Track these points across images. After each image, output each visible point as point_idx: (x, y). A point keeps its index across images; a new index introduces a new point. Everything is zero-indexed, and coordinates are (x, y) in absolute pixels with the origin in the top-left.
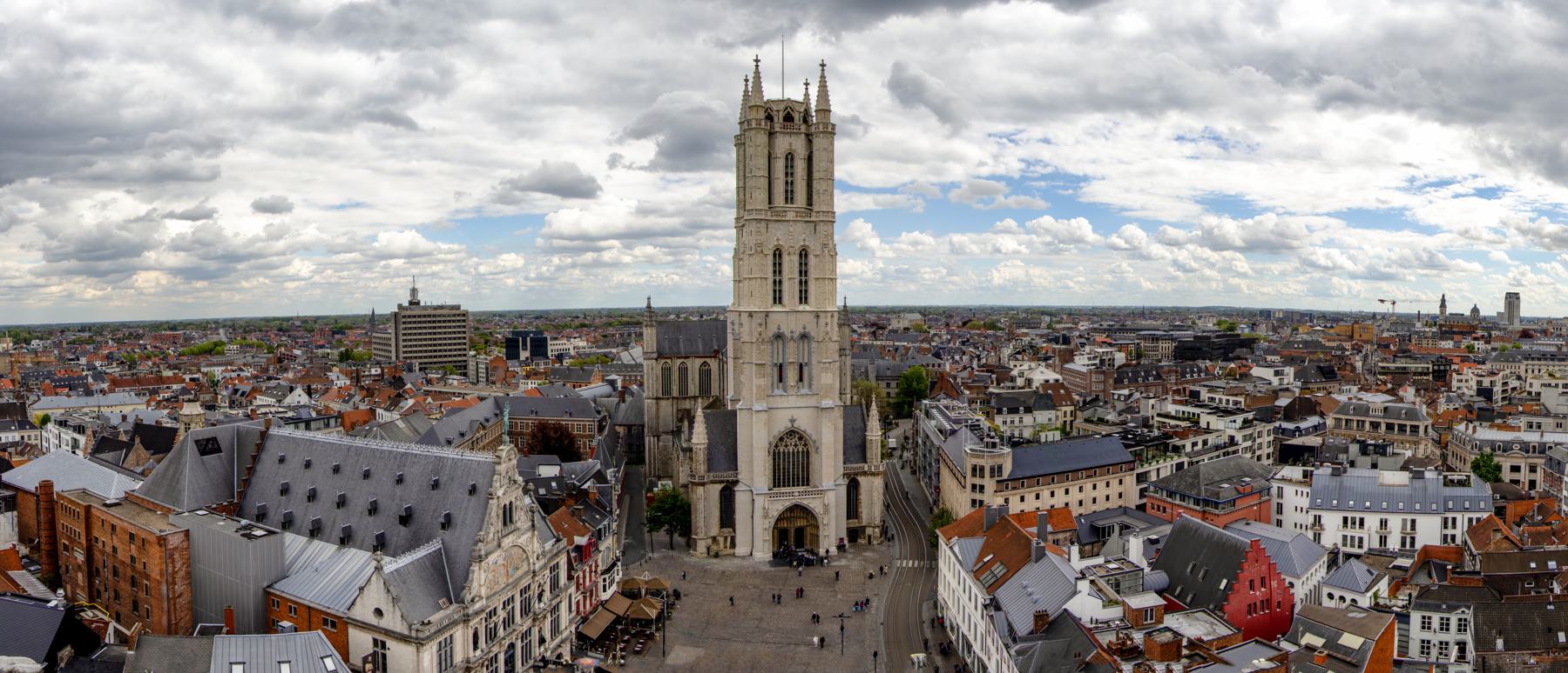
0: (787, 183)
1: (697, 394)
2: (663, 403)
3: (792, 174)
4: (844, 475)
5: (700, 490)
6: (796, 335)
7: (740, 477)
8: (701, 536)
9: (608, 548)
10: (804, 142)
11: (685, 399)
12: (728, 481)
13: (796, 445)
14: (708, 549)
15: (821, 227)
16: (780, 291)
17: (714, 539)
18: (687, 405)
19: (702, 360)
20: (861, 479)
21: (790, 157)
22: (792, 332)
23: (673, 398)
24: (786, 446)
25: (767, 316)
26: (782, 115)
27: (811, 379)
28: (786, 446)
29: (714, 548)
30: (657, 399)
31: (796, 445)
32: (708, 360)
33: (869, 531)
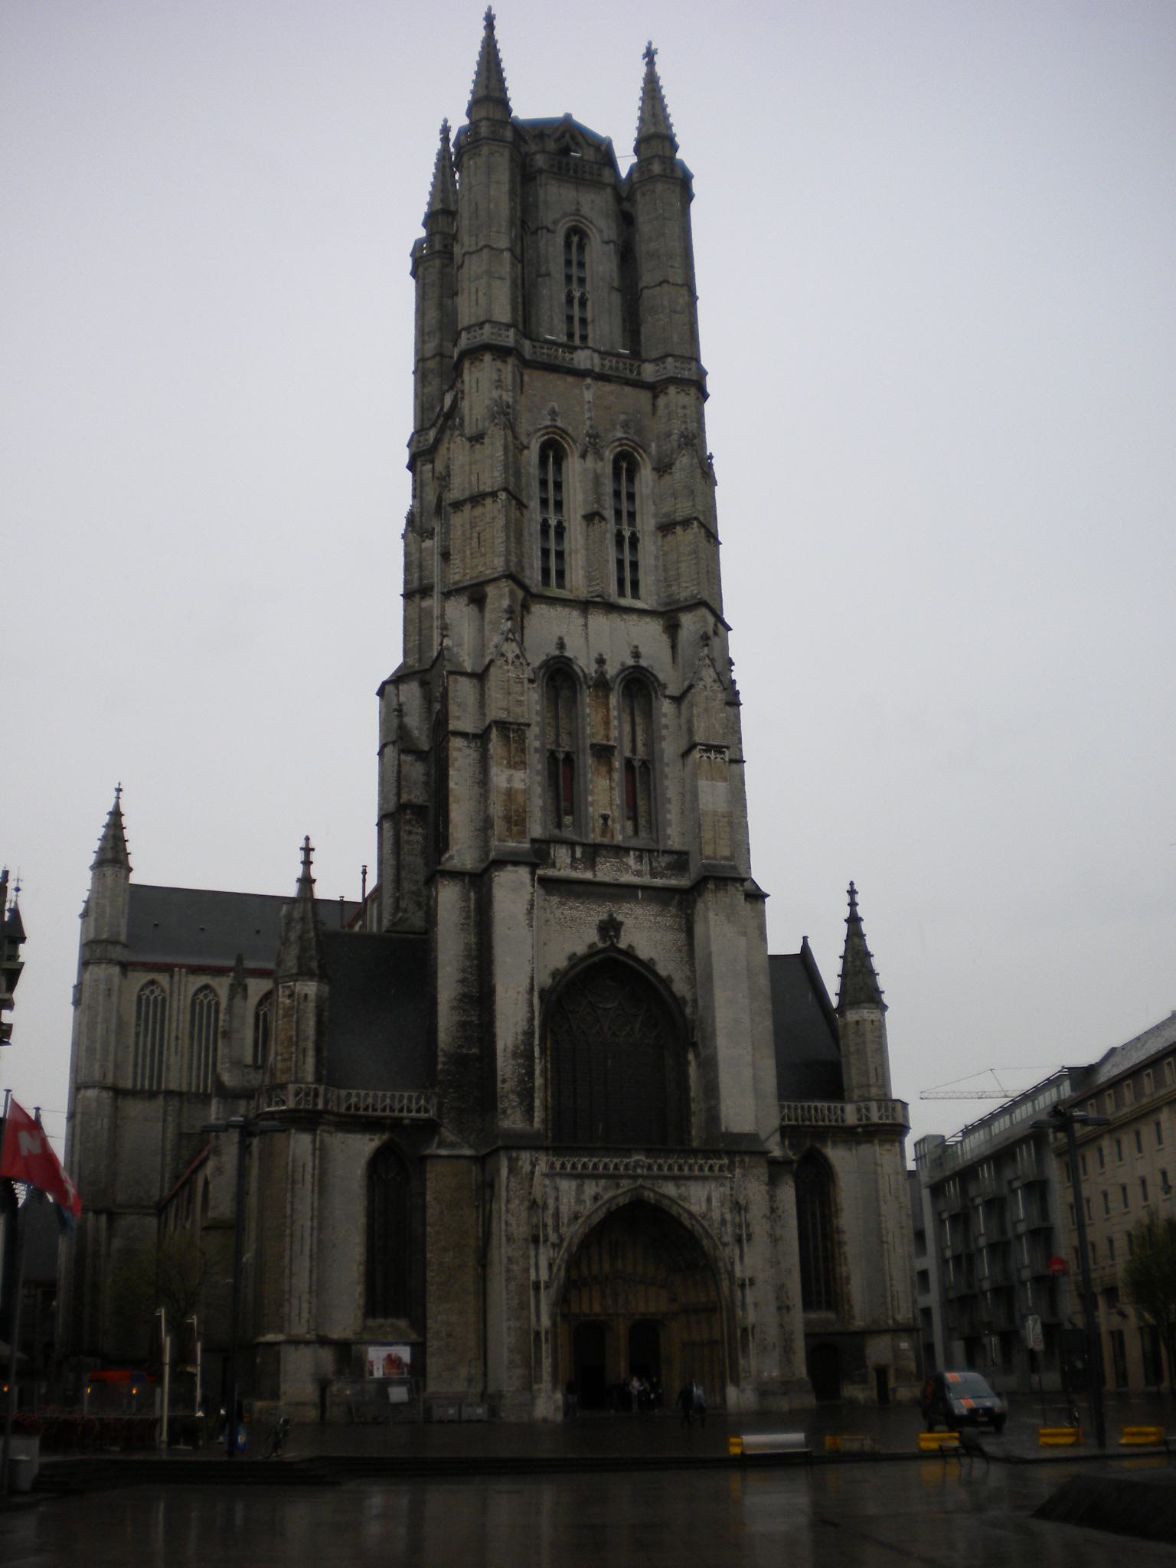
0: (570, 300)
2: (135, 1109)
3: (582, 281)
4: (784, 1131)
5: (301, 1144)
6: (611, 670)
8: (300, 1329)
12: (396, 1125)
14: (323, 1386)
15: (674, 396)
16: (560, 555)
20: (838, 1156)
21: (577, 236)
22: (601, 661)
23: (169, 1094)
25: (525, 608)
33: (878, 1351)
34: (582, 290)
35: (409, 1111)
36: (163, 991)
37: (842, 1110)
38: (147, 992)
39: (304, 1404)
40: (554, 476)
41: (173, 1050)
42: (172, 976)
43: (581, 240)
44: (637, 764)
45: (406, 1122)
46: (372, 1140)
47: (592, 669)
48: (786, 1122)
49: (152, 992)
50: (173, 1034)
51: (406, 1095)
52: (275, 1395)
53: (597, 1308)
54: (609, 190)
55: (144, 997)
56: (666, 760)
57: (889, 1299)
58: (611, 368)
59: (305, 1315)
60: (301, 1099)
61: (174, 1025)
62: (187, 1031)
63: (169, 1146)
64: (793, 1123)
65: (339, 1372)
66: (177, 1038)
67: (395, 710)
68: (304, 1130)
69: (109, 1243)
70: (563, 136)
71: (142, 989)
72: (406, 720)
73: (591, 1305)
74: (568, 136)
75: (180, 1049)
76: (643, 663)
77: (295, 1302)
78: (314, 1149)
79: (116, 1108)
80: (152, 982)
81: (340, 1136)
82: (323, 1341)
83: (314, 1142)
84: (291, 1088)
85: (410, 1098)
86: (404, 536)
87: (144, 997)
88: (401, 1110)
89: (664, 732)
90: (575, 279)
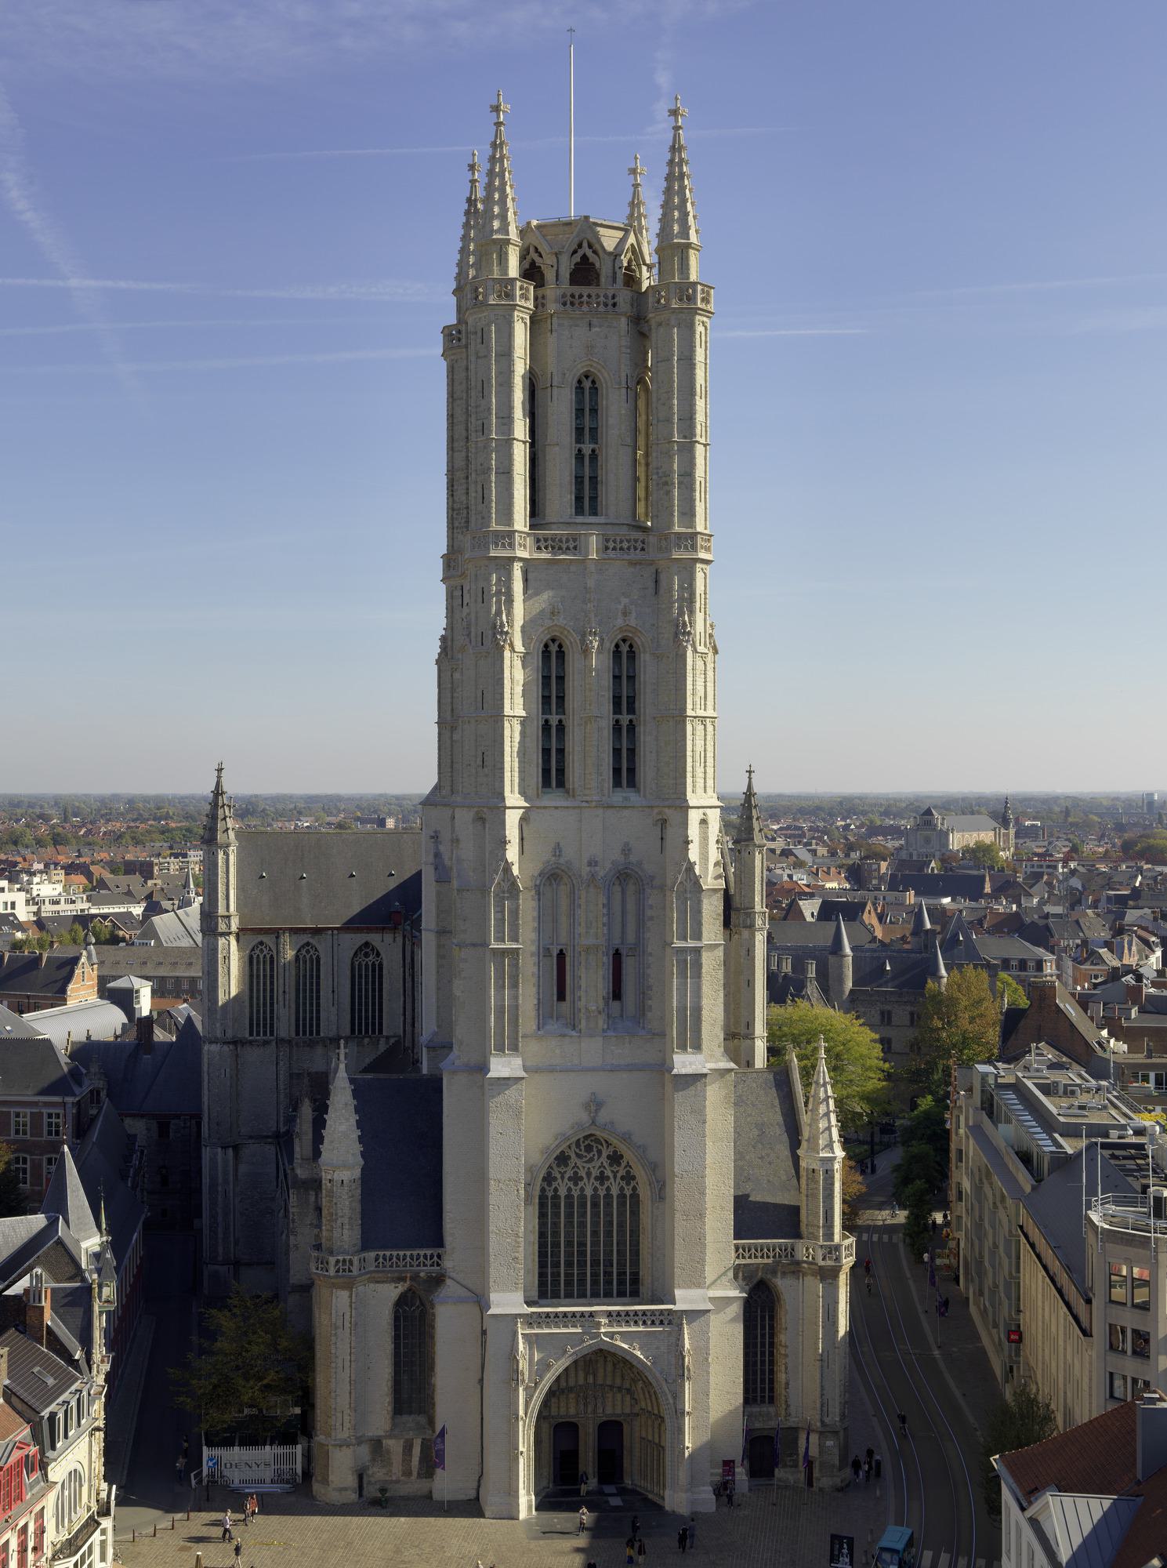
1: (347, 1031)
2: (252, 1055)
3: (594, 431)
7: (448, 1264)
8: (344, 1434)
9: (74, 1475)
11: (311, 1044)
17: (377, 1445)
18: (315, 1061)
19: (360, 939)
23: (280, 1041)
24: (576, 1179)
26: (566, 267)
27: (643, 993)
29: (378, 1473)
30: (236, 1042)
31: (602, 1178)
32: (375, 939)
34: (592, 446)
35: (426, 1266)
36: (270, 950)
38: (257, 952)
39: (346, 1489)
40: (557, 671)
41: (281, 1003)
42: (277, 938)
43: (593, 382)
45: (422, 1274)
46: (397, 1287)
47: (585, 870)
49: (261, 950)
50: (281, 991)
51: (422, 1253)
52: (325, 1481)
55: (255, 956)
56: (649, 950)
59: (347, 1425)
60: (339, 1269)
61: (281, 981)
62: (293, 983)
63: (282, 1087)
65: (373, 1460)
66: (284, 992)
67: (432, 837)
68: (343, 1288)
69: (236, 1170)
70: (580, 246)
71: (253, 950)
72: (442, 848)
74: (585, 244)
75: (287, 1003)
76: (633, 859)
77: (339, 1415)
78: (351, 1302)
79: (237, 1056)
80: (261, 943)
81: (372, 1285)
82: (360, 1441)
83: (351, 1297)
84: (332, 1260)
85: (425, 1256)
86: (438, 662)
87: (255, 956)
88: (418, 1265)
89: (649, 924)
90: (587, 430)
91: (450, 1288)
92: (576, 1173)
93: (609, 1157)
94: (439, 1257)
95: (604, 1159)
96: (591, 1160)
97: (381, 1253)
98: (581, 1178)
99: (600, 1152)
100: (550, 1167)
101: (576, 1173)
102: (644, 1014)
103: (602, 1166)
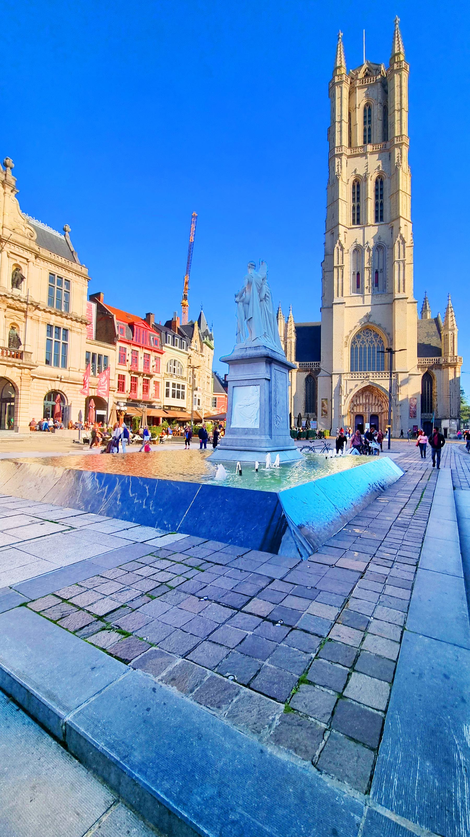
0: (365, 130)
7: (321, 366)
10: (380, 90)
13: (372, 342)
28: (363, 342)
31: (372, 342)
37: (439, 360)
44: (379, 271)
48: (420, 364)
51: (313, 363)
53: (361, 411)
54: (379, 84)
57: (449, 410)
58: (376, 149)
64: (422, 364)
73: (360, 410)
89: (387, 260)
91: (322, 373)
92: (363, 340)
93: (374, 335)
94: (319, 364)
95: (372, 336)
96: (368, 336)
97: (301, 363)
98: (365, 342)
99: (371, 334)
100: (354, 339)
101: (363, 340)
102: (386, 288)
103: (372, 338)
